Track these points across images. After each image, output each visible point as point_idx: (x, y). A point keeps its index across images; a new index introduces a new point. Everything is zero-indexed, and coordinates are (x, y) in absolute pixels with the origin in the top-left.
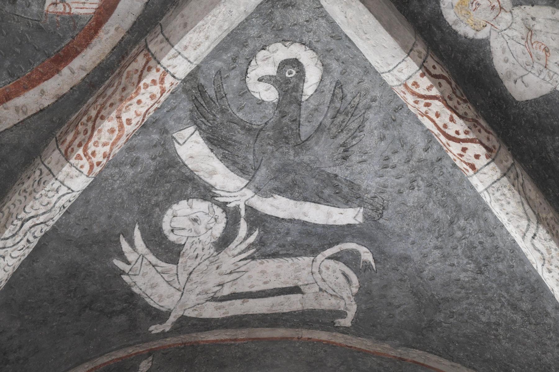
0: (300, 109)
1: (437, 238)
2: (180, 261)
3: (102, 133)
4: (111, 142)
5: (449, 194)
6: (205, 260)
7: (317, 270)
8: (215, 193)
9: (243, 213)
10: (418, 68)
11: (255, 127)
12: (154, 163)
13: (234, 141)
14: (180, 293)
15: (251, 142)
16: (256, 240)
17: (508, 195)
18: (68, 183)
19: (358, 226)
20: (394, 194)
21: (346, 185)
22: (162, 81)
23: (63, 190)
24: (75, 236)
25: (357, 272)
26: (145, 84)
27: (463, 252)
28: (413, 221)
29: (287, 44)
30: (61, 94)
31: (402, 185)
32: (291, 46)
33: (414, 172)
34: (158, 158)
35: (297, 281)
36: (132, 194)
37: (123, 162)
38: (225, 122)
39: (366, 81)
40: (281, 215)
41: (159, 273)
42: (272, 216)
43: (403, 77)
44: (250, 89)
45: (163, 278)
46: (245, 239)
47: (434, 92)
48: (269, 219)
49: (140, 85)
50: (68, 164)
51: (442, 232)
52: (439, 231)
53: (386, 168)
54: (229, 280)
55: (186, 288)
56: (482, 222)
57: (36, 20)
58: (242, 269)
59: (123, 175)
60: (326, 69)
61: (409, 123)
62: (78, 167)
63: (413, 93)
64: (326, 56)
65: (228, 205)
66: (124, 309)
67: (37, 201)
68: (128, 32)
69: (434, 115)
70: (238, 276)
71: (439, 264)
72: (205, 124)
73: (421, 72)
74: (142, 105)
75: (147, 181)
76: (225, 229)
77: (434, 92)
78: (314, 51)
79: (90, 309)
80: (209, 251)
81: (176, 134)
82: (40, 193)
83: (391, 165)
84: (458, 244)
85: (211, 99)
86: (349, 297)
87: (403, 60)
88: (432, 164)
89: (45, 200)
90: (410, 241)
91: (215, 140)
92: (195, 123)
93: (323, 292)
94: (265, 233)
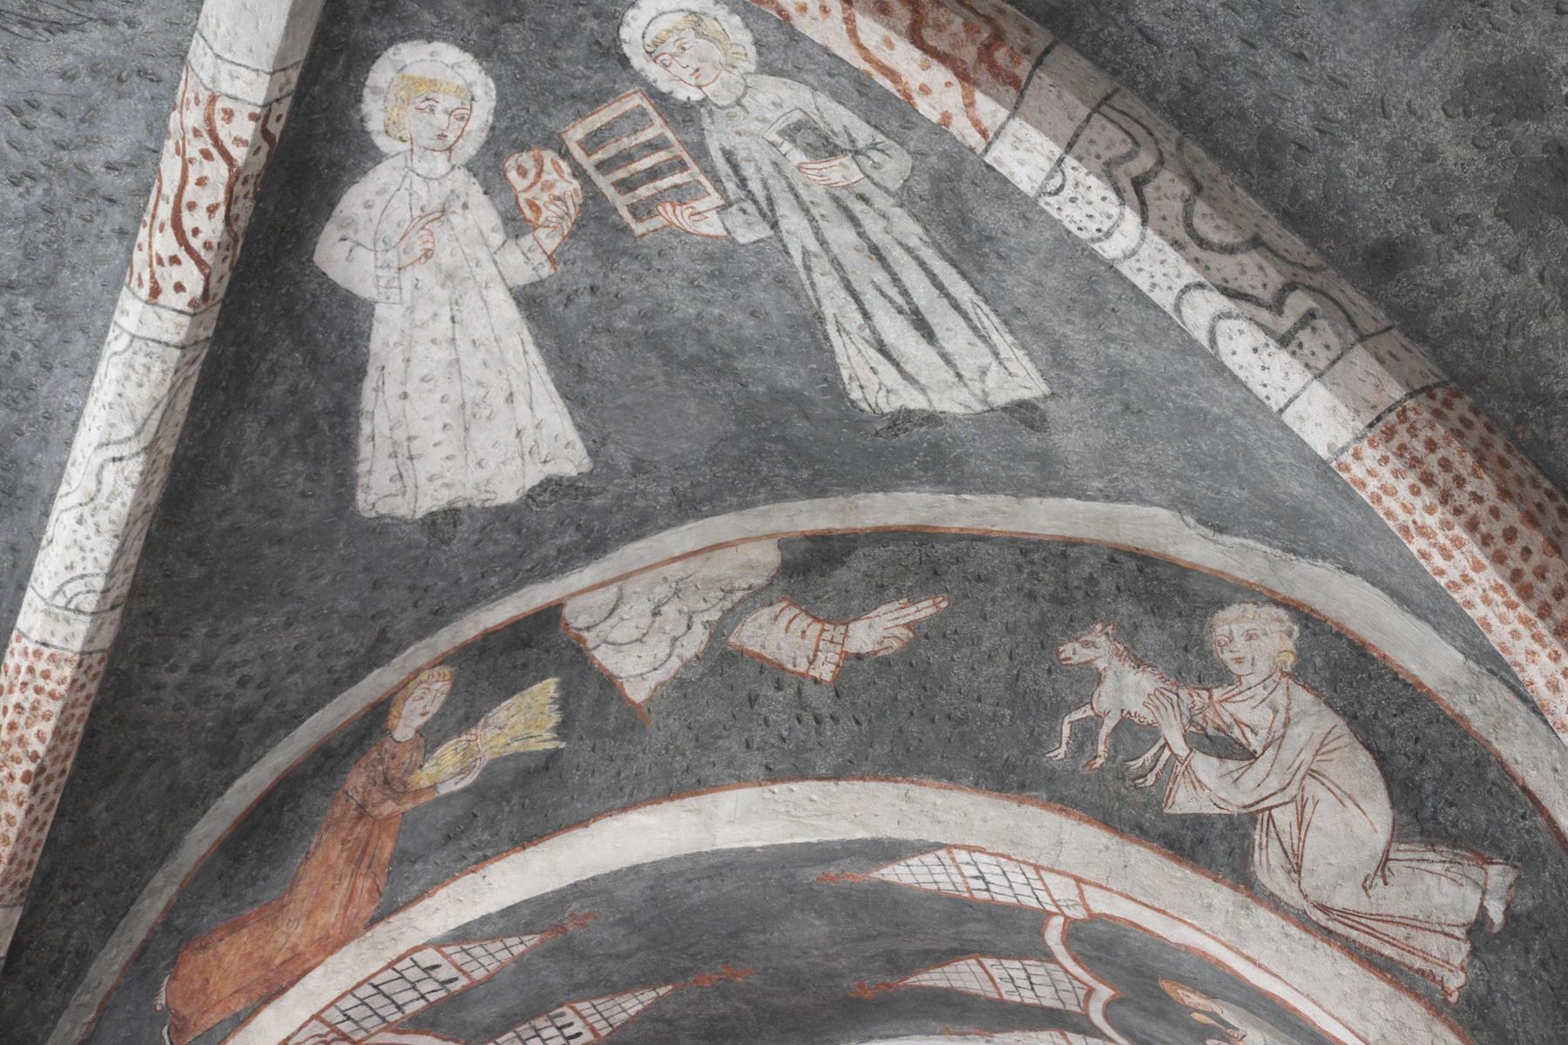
10: (261, 102)
43: (225, 86)
47: (239, 154)
61: (137, 111)
63: (209, 119)
69: (197, 177)
73: (258, 111)
77: (239, 154)
87: (257, 71)
88: (93, 192)
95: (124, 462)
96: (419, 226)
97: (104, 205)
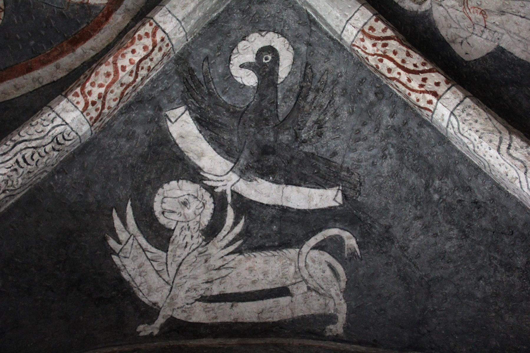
0: (277, 91)
1: (416, 206)
2: (170, 249)
3: (99, 76)
4: (106, 84)
5: (420, 156)
6: (194, 250)
7: (304, 265)
8: (203, 176)
9: (229, 199)
11: (238, 109)
12: (148, 139)
13: (220, 123)
14: (169, 287)
15: (235, 124)
16: (243, 230)
17: (474, 114)
18: (63, 115)
19: (339, 208)
20: (369, 168)
21: (323, 163)
22: (154, 34)
23: (58, 121)
25: (342, 261)
26: (139, 35)
27: (443, 217)
28: (390, 192)
29: (263, 33)
30: (73, 68)
31: (374, 156)
32: (267, 35)
33: (384, 140)
34: (152, 134)
35: (285, 280)
37: (121, 134)
38: (212, 105)
39: (331, 60)
40: (265, 201)
41: (149, 260)
42: (257, 202)
43: (360, 25)
44: (233, 74)
45: (153, 266)
46: (232, 228)
48: (254, 206)
49: (135, 36)
50: (66, 99)
51: (420, 199)
52: (416, 198)
53: (358, 141)
55: (175, 282)
56: (456, 177)
57: (60, 8)
58: (231, 265)
60: (297, 53)
62: (75, 103)
63: (371, 37)
64: (296, 41)
65: (216, 190)
67: (32, 128)
68: (132, 19)
69: (392, 53)
70: (226, 273)
71: (422, 237)
72: (194, 105)
73: (374, 17)
74: (135, 54)
75: (141, 156)
77: (389, 33)
78: (285, 38)
80: (197, 240)
81: (169, 112)
82: (36, 121)
83: (362, 137)
84: (437, 209)
85: (200, 82)
86: (338, 295)
87: (358, 9)
89: (40, 128)
90: (390, 216)
91: (203, 121)
92: (185, 103)
93: (311, 291)
95: (512, 144)
96: (468, 11)
97: (407, 127)
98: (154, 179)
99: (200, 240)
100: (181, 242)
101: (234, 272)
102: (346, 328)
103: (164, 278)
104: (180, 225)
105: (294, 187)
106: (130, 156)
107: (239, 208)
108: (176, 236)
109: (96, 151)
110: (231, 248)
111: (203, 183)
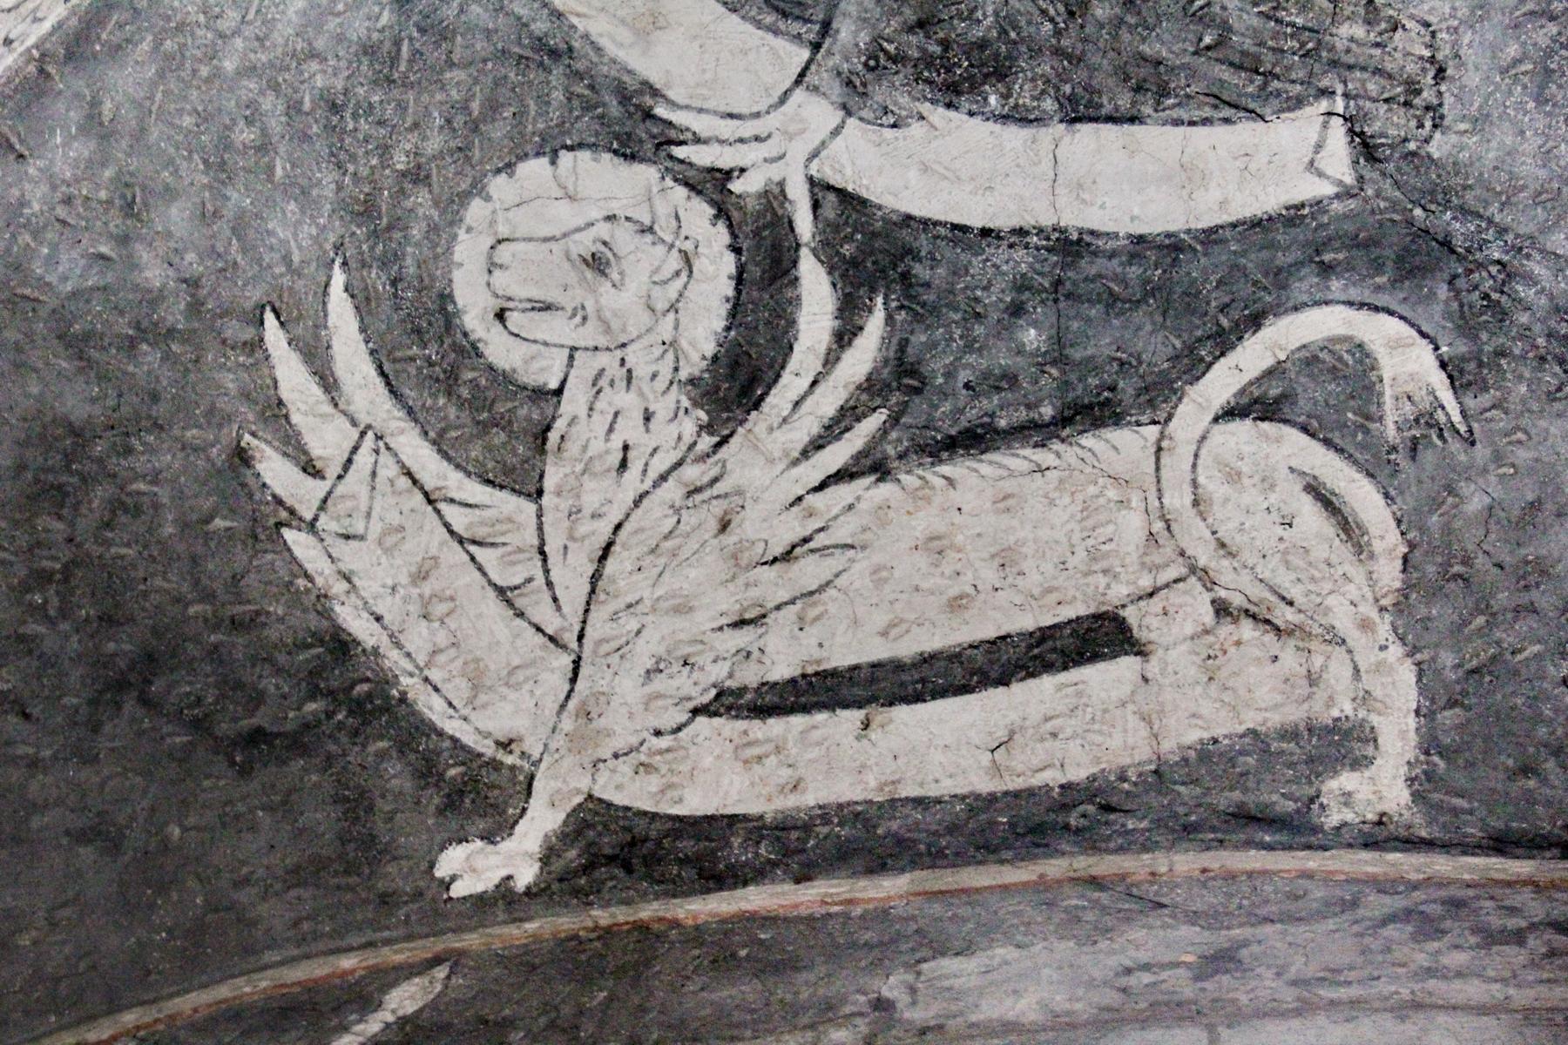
2: (549, 483)
6: (663, 478)
7: (1188, 499)
9: (804, 225)
14: (566, 660)
19: (1337, 207)
24: (51, 278)
35: (1102, 581)
36: (307, 114)
42: (936, 223)
45: (480, 569)
48: (923, 243)
54: (786, 597)
58: (840, 534)
59: (258, 11)
65: (736, 186)
66: (307, 726)
70: (826, 575)
75: (368, 50)
76: (736, 310)
79: (145, 701)
80: (673, 430)
86: (1365, 625)
93: (1236, 621)
94: (917, 317)
98: (440, 156)
99: (688, 427)
100: (597, 446)
101: (857, 567)
102: (1423, 784)
103: (536, 620)
104: (586, 366)
105: (1110, 133)
106: (313, 55)
107: (854, 263)
108: (573, 421)
109: (150, 38)
110: (837, 455)
111: (671, 157)
